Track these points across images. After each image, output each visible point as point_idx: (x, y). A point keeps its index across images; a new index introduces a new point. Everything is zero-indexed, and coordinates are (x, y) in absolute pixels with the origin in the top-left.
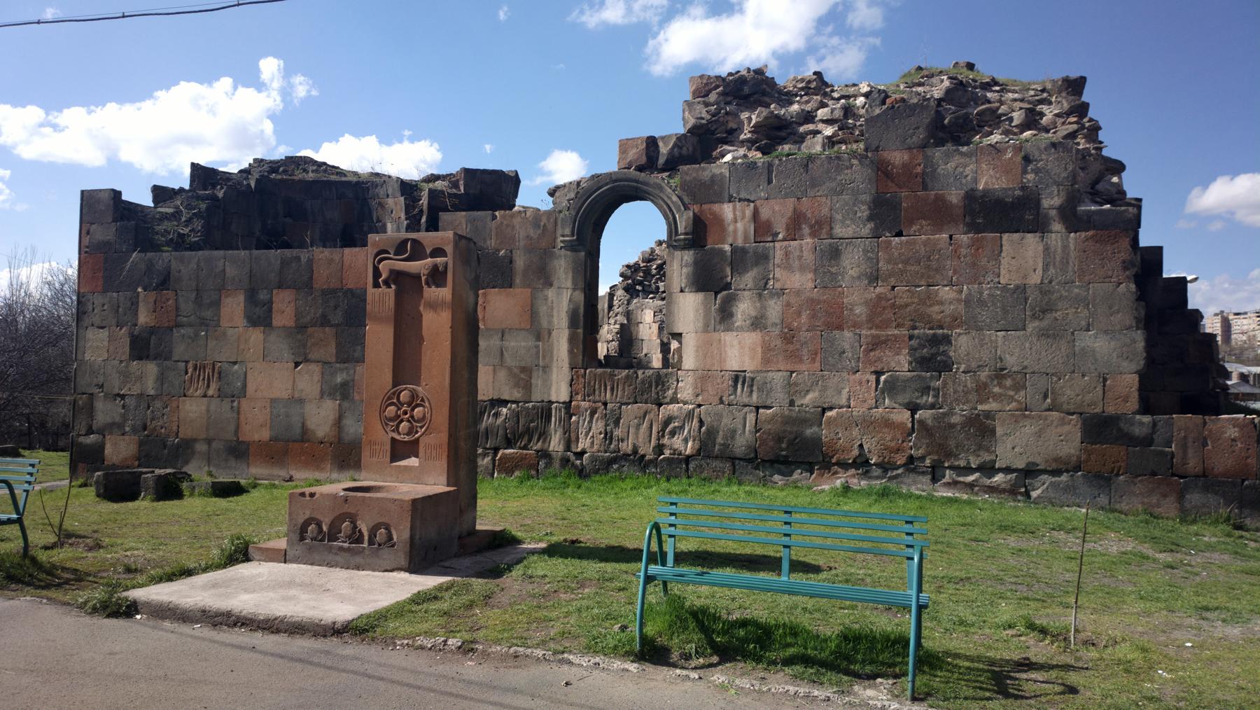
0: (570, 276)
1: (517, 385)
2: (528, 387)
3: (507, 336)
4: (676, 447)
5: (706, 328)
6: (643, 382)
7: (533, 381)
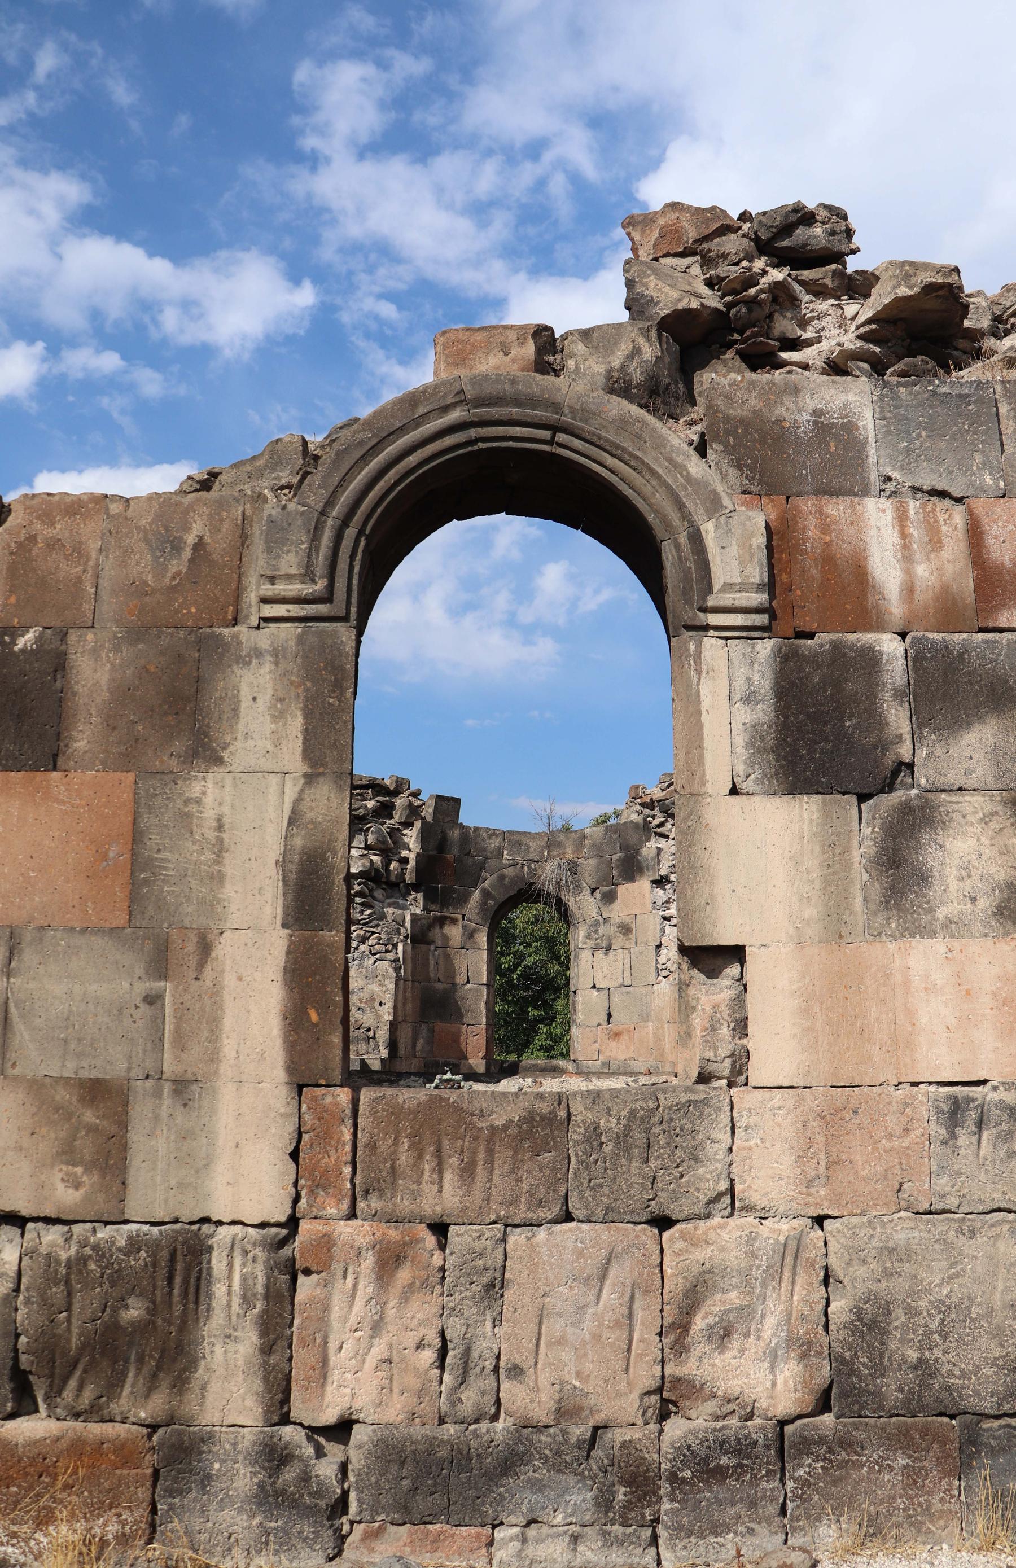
0: (296, 723)
1: (67, 1153)
2: (111, 1160)
3: (29, 956)
4: (733, 1385)
5: (836, 933)
6: (594, 1132)
7: (136, 1137)
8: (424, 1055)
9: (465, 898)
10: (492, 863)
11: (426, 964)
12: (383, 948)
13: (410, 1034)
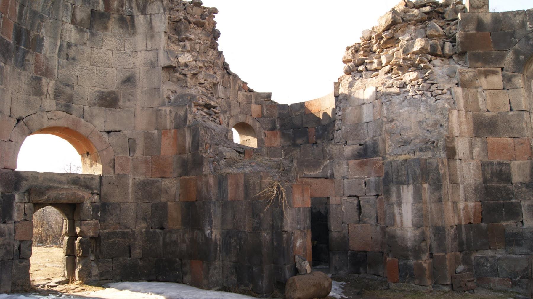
8: (480, 158)
9: (502, 57)
10: (520, 33)
11: (476, 101)
12: (440, 92)
13: (467, 144)
